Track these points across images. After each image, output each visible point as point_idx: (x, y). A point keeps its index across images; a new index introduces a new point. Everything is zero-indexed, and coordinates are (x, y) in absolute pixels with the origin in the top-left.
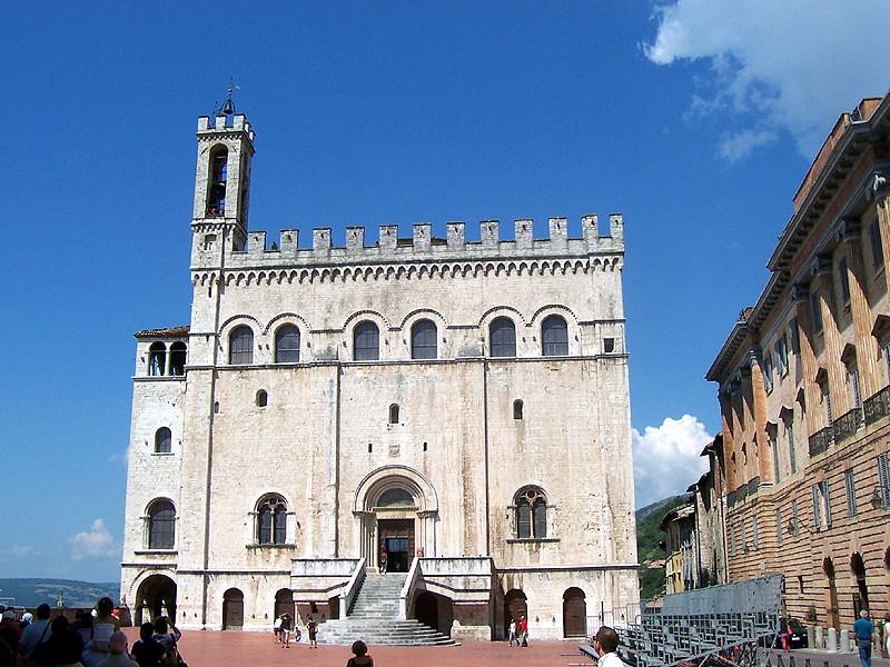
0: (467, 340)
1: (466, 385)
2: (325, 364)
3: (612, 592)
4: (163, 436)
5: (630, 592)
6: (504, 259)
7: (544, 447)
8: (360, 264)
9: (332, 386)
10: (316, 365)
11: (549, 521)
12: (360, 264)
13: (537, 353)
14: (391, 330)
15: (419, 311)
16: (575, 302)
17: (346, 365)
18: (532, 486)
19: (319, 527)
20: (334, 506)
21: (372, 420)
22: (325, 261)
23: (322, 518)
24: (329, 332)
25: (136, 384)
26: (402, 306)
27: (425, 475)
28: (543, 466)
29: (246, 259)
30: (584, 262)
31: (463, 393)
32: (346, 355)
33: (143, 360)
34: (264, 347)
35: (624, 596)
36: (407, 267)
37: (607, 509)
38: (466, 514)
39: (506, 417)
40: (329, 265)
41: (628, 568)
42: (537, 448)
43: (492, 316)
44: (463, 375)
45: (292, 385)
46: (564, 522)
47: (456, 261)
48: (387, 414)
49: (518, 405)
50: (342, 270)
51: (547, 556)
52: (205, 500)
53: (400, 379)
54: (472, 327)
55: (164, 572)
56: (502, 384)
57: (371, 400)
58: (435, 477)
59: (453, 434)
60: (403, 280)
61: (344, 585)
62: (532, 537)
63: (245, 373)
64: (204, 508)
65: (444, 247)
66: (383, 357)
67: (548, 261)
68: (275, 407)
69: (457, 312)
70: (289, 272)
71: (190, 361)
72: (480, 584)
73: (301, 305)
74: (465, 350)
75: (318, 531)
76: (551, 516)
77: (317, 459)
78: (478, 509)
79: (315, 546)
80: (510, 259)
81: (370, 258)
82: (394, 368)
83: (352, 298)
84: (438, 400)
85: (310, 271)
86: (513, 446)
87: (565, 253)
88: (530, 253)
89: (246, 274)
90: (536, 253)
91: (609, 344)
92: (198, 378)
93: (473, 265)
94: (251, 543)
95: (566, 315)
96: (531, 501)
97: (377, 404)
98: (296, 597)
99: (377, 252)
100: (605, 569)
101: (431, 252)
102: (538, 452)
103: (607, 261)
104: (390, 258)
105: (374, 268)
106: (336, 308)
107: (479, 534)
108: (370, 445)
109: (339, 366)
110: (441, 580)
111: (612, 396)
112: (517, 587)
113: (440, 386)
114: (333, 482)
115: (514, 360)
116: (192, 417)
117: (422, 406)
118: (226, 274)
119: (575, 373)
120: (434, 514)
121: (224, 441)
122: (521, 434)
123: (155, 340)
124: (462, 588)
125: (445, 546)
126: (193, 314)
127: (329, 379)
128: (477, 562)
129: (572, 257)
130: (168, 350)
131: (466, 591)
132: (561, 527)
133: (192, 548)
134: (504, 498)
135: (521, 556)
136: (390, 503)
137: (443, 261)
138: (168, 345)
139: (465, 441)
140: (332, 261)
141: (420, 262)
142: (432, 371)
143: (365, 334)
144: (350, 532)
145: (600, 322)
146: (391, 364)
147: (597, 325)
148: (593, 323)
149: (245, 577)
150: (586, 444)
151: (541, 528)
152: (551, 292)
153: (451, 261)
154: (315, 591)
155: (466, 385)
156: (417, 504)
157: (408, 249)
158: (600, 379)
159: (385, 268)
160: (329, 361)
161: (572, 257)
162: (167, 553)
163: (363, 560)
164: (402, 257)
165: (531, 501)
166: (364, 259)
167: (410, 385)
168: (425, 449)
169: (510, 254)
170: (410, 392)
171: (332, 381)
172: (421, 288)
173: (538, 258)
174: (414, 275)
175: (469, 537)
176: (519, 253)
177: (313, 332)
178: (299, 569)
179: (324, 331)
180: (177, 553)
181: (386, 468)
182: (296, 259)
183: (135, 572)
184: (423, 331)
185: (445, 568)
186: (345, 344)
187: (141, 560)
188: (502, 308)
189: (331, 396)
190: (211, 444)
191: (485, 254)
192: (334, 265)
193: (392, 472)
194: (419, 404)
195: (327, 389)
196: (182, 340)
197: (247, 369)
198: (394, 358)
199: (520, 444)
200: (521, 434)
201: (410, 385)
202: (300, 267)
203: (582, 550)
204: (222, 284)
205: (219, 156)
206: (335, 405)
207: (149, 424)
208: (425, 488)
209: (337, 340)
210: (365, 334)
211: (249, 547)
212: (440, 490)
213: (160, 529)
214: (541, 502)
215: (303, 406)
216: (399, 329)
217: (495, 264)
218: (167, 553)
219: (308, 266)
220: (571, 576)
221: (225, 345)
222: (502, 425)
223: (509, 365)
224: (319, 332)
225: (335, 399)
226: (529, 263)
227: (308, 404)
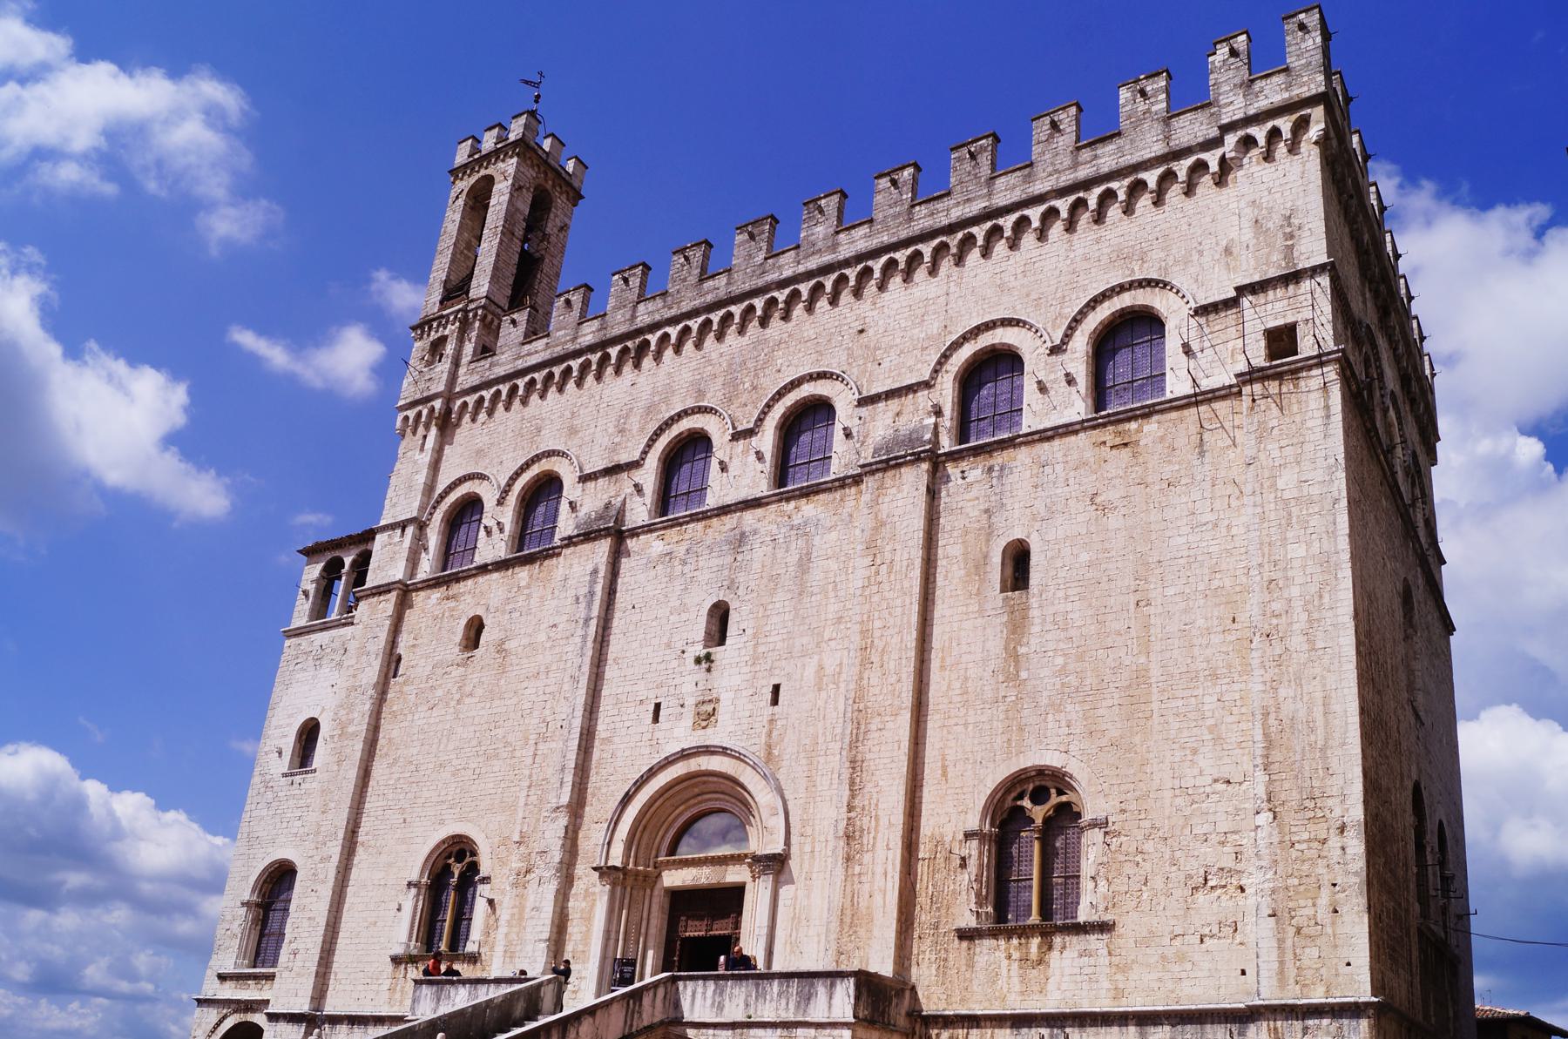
0: (903, 420)
4: (309, 734)
7: (1080, 658)
9: (593, 582)
11: (1087, 867)
17: (634, 532)
18: (1041, 772)
21: (668, 646)
25: (287, 643)
27: (768, 767)
28: (1073, 710)
31: (871, 547)
32: (639, 512)
33: (306, 593)
34: (495, 529)
37: (1264, 818)
39: (978, 593)
42: (1060, 661)
44: (876, 501)
45: (529, 596)
46: (1128, 869)
48: (699, 627)
53: (740, 541)
54: (911, 389)
56: (974, 511)
57: (675, 603)
58: (791, 772)
59: (838, 656)
68: (492, 649)
71: (372, 580)
82: (730, 521)
83: (669, 391)
84: (816, 576)
96: (1038, 813)
97: (683, 608)
102: (1063, 671)
104: (747, 287)
106: (634, 423)
108: (658, 706)
113: (824, 542)
114: (565, 799)
117: (781, 596)
118: (459, 402)
121: (395, 734)
122: (1017, 625)
126: (390, 493)
132: (1120, 885)
134: (956, 812)
139: (865, 663)
146: (724, 510)
167: (758, 554)
168: (775, 702)
177: (585, 478)
181: (684, 755)
183: (212, 1015)
187: (229, 991)
193: (695, 764)
195: (584, 590)
203: (1181, 958)
204: (446, 424)
205: (479, 199)
206: (594, 623)
207: (290, 716)
209: (625, 482)
212: (800, 804)
214: (1066, 816)
216: (750, 433)
221: (433, 538)
222: (969, 618)
223: (999, 459)
225: (595, 611)
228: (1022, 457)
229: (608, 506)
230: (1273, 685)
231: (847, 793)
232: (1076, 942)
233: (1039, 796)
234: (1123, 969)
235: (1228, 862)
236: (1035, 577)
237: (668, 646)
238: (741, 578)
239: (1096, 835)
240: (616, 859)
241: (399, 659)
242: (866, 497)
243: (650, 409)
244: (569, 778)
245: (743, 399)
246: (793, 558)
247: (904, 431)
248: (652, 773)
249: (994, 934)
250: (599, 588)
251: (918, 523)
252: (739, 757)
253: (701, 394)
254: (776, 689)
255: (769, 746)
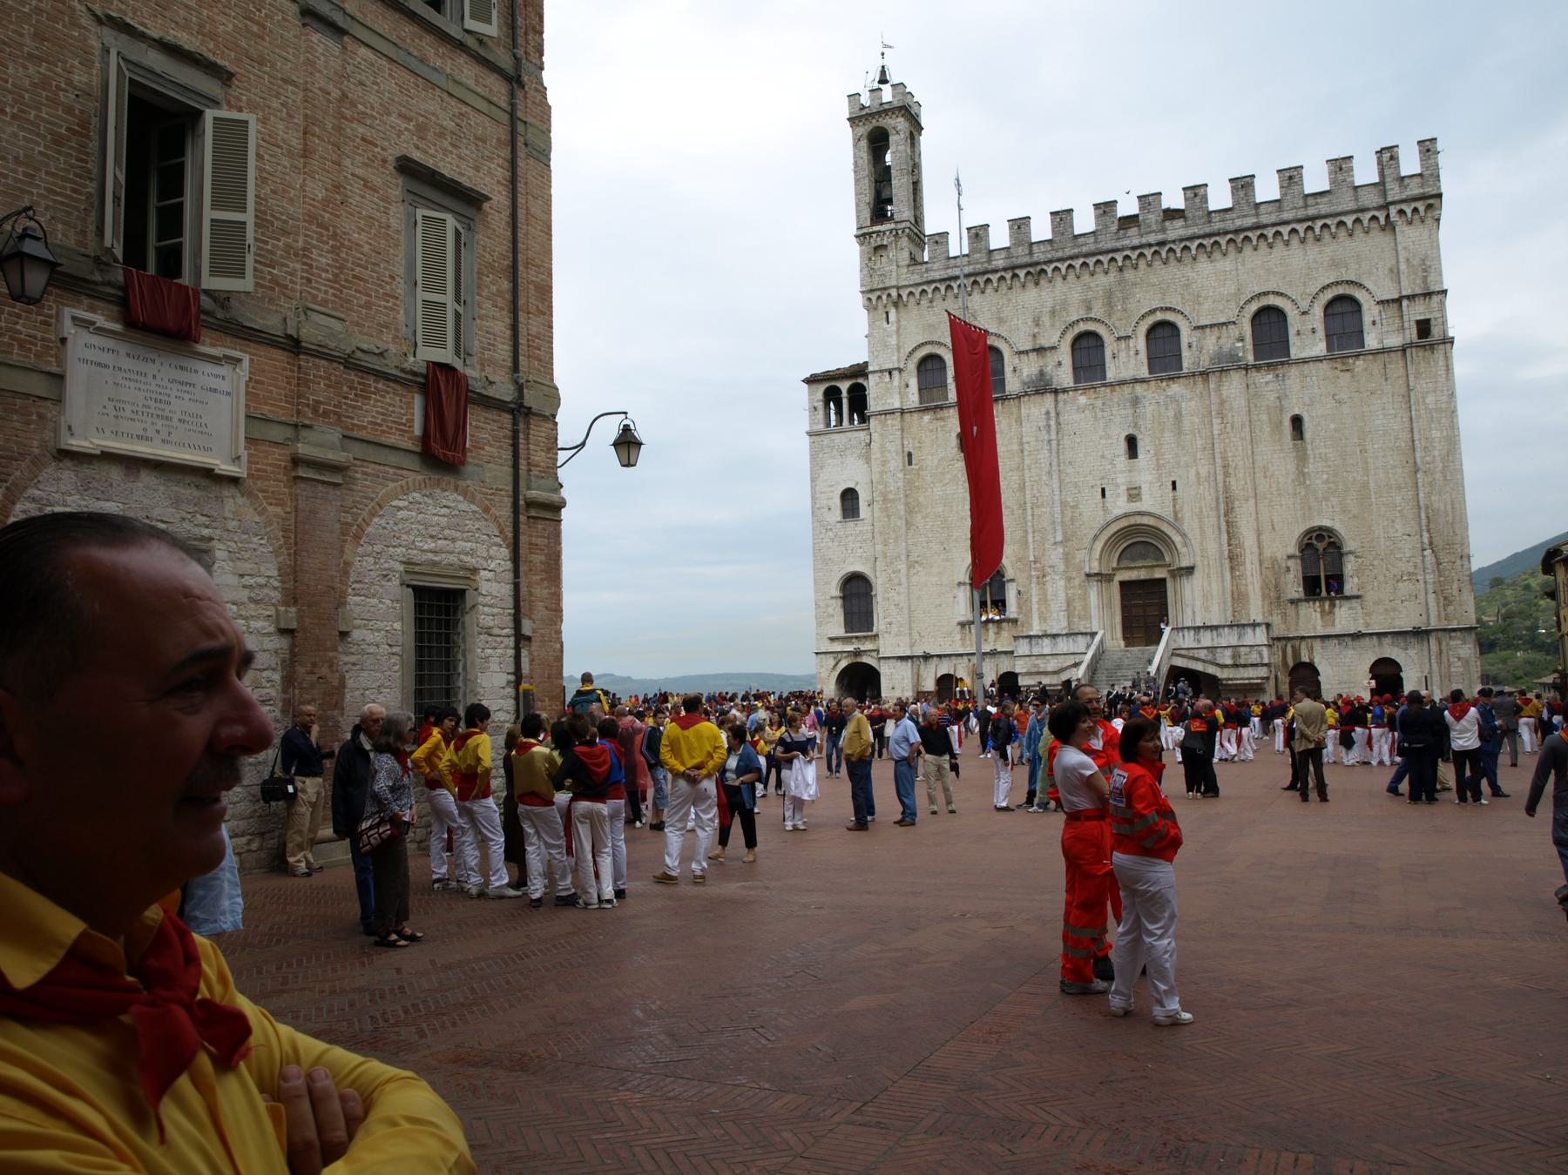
0: (1222, 341)
1: (1222, 402)
2: (1037, 392)
3: (1440, 663)
4: (849, 496)
5: (1466, 662)
6: (1265, 226)
8: (1072, 258)
9: (1048, 419)
10: (1026, 394)
12: (1072, 258)
13: (1320, 348)
14: (1119, 339)
15: (1153, 311)
16: (1371, 273)
17: (1065, 391)
18: (1320, 528)
19: (1045, 595)
20: (1062, 568)
21: (1103, 457)
22: (1026, 260)
23: (1048, 586)
24: (1040, 350)
26: (1131, 306)
28: (1334, 500)
29: (927, 271)
30: (1381, 216)
31: (1221, 414)
32: (1065, 377)
35: (1457, 668)
36: (1134, 255)
37: (1427, 552)
38: (1232, 569)
40: (1031, 265)
41: (1460, 630)
43: (1254, 307)
44: (1218, 388)
47: (1198, 237)
48: (1122, 447)
49: (1297, 422)
50: (1049, 269)
51: (1345, 618)
52: (904, 571)
53: (1136, 402)
55: (865, 659)
58: (1190, 524)
60: (1129, 274)
61: (1076, 665)
62: (1324, 594)
63: (940, 414)
64: (904, 580)
65: (1180, 223)
66: (1111, 375)
67: (1328, 221)
69: (1206, 306)
70: (981, 280)
71: (873, 405)
72: (1254, 658)
73: (1001, 321)
74: (1218, 357)
75: (1044, 599)
76: (1349, 566)
77: (1037, 511)
78: (1248, 562)
79: (1043, 618)
80: (1274, 225)
81: (1084, 249)
82: (1127, 389)
83: (1065, 304)
84: (1186, 425)
85: (1008, 276)
86: (1292, 477)
87: (1352, 206)
88: (1301, 214)
89: (929, 289)
90: (1311, 212)
91: (1424, 328)
92: (884, 424)
93: (1223, 241)
94: (962, 619)
95: (1360, 295)
98: (1022, 682)
99: (1092, 240)
100: (1428, 632)
101: (1163, 230)
102: (1327, 482)
103: (1415, 210)
104: (1109, 246)
105: (1091, 261)
106: (1046, 319)
107: (1252, 595)
108: (1103, 490)
109: (1056, 392)
110: (1202, 654)
111: (1430, 399)
112: (1305, 659)
115: (1287, 363)
116: (882, 473)
117: (1167, 434)
119: (1376, 372)
120: (1190, 570)
121: (921, 499)
122: (1302, 458)
123: (826, 385)
124: (1229, 662)
125: (1207, 609)
127: (1043, 410)
128: (1249, 630)
129: (1363, 210)
130: (844, 394)
131: (1236, 666)
133: (894, 629)
135: (1311, 619)
136: (1133, 559)
137: (1181, 240)
138: (844, 386)
139: (1227, 474)
140: (1035, 258)
141: (1150, 245)
142: (1176, 388)
143: (1088, 351)
144: (1085, 597)
145: (1408, 297)
146: (1122, 383)
147: (1405, 303)
148: (1398, 301)
149: (960, 660)
150: (1394, 467)
151: (1336, 582)
152: (1335, 264)
153: (1191, 238)
154: (1045, 673)
155: (1222, 402)
156: (1168, 559)
157: (1133, 231)
158: (1411, 378)
159: (1105, 259)
160: (1042, 387)
161: (1363, 210)
162: (865, 637)
163: (1100, 633)
164: (1126, 242)
165: (1320, 546)
166: (1076, 251)
167: (1148, 409)
169: (1273, 218)
170: (1149, 416)
171: (1048, 413)
172: (1154, 280)
173: (1313, 219)
174: (1142, 264)
175: (1239, 598)
176: (1286, 216)
178: (1023, 648)
179: (1034, 350)
180: (876, 636)
181: (1126, 516)
182: (989, 261)
184: (1163, 337)
185: (1207, 639)
186: (1060, 364)
187: (837, 647)
188: (1265, 294)
189: (1049, 432)
190: (907, 504)
191: (1238, 223)
192: (1037, 263)
193: (1132, 521)
194: (1162, 431)
195: (1042, 424)
196: (860, 381)
197: (941, 408)
198: (1127, 374)
199: (1301, 476)
200: (1302, 458)
201: (1149, 409)
202: (995, 271)
203: (1394, 609)
208: (1177, 539)
209: (1050, 361)
210: (1088, 351)
211: (962, 625)
212: (1198, 542)
213: (855, 609)
215: (1015, 447)
217: (1253, 235)
218: (865, 637)
219: (1005, 269)
220: (1380, 644)
224: (1026, 352)
225: (1053, 436)
226: (1301, 228)
227: (1021, 443)
228: (1294, 371)
229: (1042, 373)
230: (1429, 495)
231: (1225, 537)
232: (1346, 604)
233: (1320, 538)
234: (1369, 614)
235: (1411, 570)
236: (1308, 435)
237: (1103, 457)
238: (1141, 422)
239: (1351, 558)
240: (1095, 567)
241: (910, 455)
242: (1212, 386)
243: (1053, 312)
244: (1059, 528)
245: (1118, 315)
246: (1171, 414)
247: (1226, 349)
248: (1108, 525)
249: (1307, 601)
250: (1053, 423)
251: (1243, 403)
252: (1159, 518)
253: (1089, 309)
254: (1174, 483)
255: (1176, 513)
